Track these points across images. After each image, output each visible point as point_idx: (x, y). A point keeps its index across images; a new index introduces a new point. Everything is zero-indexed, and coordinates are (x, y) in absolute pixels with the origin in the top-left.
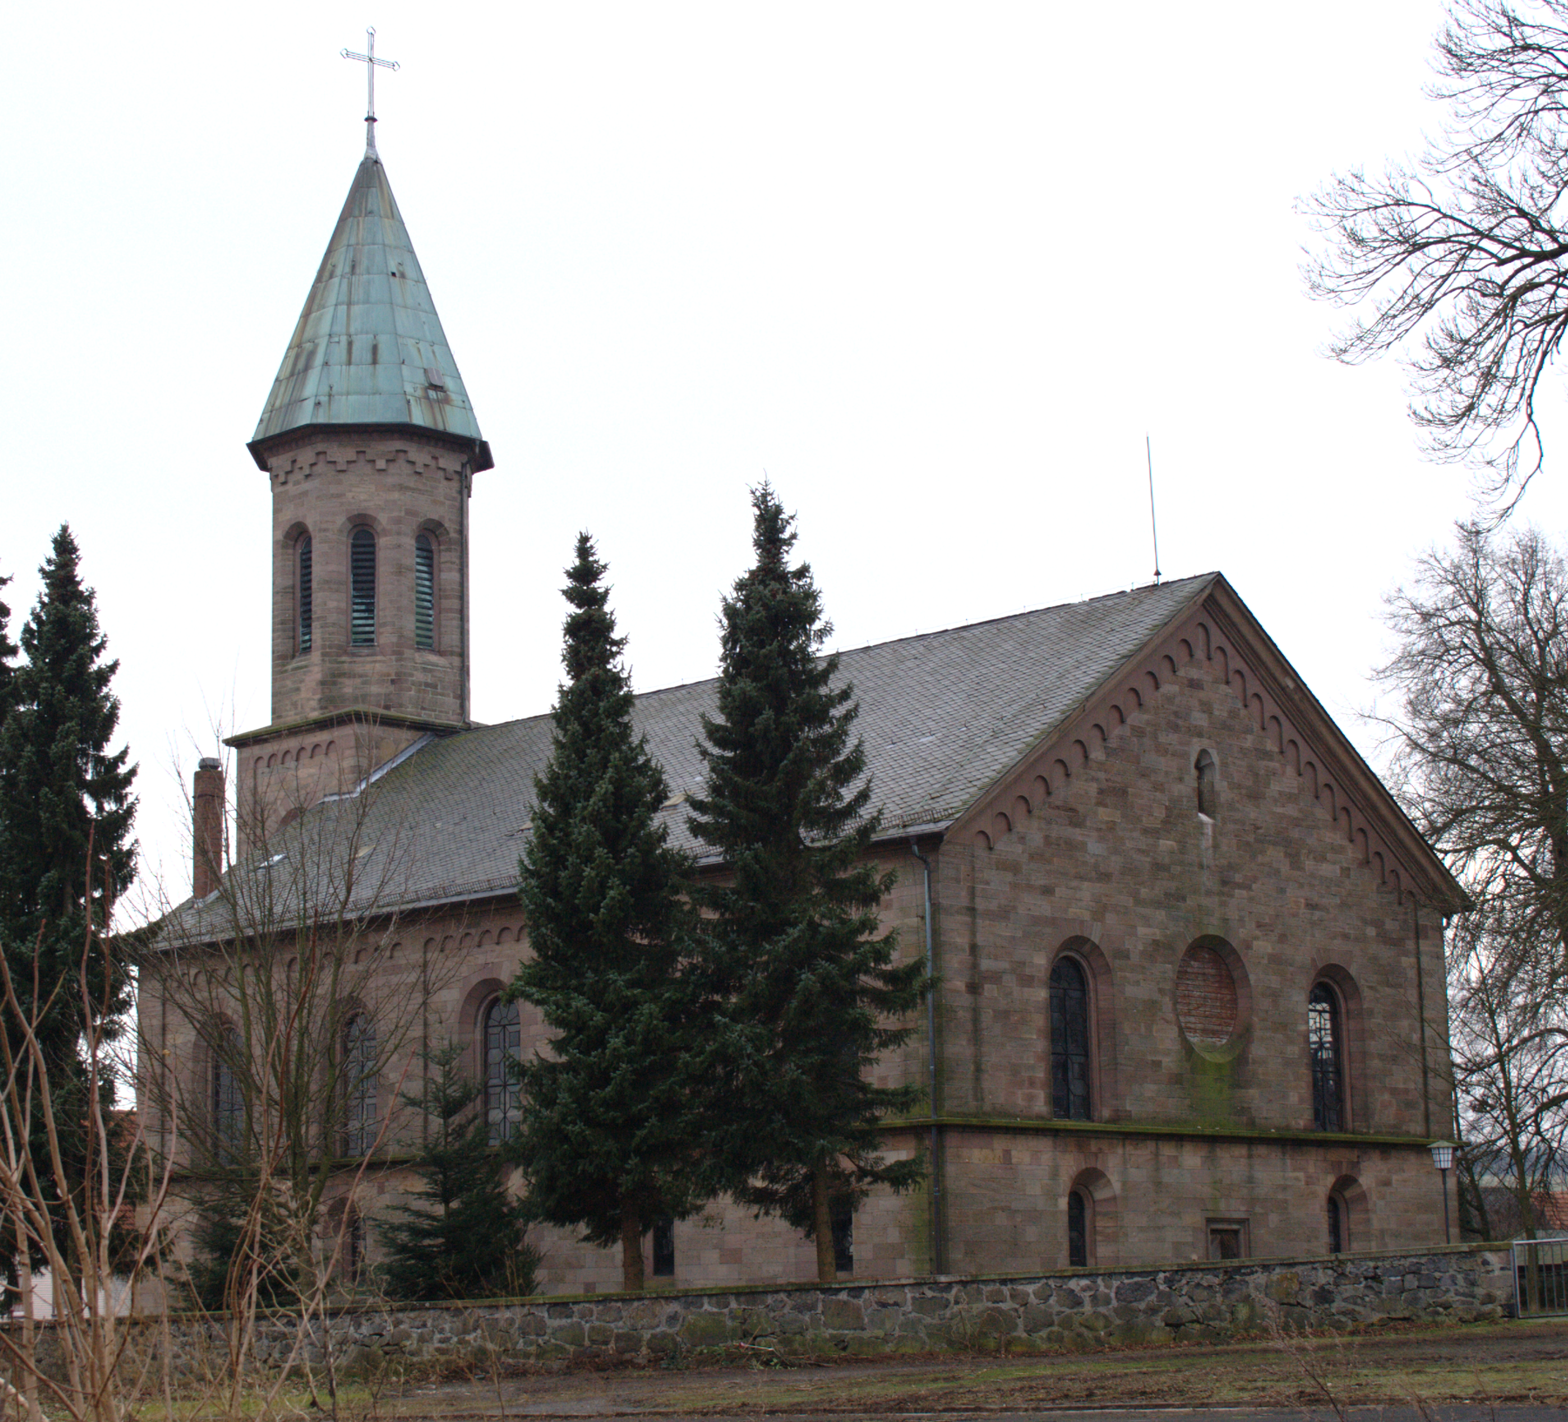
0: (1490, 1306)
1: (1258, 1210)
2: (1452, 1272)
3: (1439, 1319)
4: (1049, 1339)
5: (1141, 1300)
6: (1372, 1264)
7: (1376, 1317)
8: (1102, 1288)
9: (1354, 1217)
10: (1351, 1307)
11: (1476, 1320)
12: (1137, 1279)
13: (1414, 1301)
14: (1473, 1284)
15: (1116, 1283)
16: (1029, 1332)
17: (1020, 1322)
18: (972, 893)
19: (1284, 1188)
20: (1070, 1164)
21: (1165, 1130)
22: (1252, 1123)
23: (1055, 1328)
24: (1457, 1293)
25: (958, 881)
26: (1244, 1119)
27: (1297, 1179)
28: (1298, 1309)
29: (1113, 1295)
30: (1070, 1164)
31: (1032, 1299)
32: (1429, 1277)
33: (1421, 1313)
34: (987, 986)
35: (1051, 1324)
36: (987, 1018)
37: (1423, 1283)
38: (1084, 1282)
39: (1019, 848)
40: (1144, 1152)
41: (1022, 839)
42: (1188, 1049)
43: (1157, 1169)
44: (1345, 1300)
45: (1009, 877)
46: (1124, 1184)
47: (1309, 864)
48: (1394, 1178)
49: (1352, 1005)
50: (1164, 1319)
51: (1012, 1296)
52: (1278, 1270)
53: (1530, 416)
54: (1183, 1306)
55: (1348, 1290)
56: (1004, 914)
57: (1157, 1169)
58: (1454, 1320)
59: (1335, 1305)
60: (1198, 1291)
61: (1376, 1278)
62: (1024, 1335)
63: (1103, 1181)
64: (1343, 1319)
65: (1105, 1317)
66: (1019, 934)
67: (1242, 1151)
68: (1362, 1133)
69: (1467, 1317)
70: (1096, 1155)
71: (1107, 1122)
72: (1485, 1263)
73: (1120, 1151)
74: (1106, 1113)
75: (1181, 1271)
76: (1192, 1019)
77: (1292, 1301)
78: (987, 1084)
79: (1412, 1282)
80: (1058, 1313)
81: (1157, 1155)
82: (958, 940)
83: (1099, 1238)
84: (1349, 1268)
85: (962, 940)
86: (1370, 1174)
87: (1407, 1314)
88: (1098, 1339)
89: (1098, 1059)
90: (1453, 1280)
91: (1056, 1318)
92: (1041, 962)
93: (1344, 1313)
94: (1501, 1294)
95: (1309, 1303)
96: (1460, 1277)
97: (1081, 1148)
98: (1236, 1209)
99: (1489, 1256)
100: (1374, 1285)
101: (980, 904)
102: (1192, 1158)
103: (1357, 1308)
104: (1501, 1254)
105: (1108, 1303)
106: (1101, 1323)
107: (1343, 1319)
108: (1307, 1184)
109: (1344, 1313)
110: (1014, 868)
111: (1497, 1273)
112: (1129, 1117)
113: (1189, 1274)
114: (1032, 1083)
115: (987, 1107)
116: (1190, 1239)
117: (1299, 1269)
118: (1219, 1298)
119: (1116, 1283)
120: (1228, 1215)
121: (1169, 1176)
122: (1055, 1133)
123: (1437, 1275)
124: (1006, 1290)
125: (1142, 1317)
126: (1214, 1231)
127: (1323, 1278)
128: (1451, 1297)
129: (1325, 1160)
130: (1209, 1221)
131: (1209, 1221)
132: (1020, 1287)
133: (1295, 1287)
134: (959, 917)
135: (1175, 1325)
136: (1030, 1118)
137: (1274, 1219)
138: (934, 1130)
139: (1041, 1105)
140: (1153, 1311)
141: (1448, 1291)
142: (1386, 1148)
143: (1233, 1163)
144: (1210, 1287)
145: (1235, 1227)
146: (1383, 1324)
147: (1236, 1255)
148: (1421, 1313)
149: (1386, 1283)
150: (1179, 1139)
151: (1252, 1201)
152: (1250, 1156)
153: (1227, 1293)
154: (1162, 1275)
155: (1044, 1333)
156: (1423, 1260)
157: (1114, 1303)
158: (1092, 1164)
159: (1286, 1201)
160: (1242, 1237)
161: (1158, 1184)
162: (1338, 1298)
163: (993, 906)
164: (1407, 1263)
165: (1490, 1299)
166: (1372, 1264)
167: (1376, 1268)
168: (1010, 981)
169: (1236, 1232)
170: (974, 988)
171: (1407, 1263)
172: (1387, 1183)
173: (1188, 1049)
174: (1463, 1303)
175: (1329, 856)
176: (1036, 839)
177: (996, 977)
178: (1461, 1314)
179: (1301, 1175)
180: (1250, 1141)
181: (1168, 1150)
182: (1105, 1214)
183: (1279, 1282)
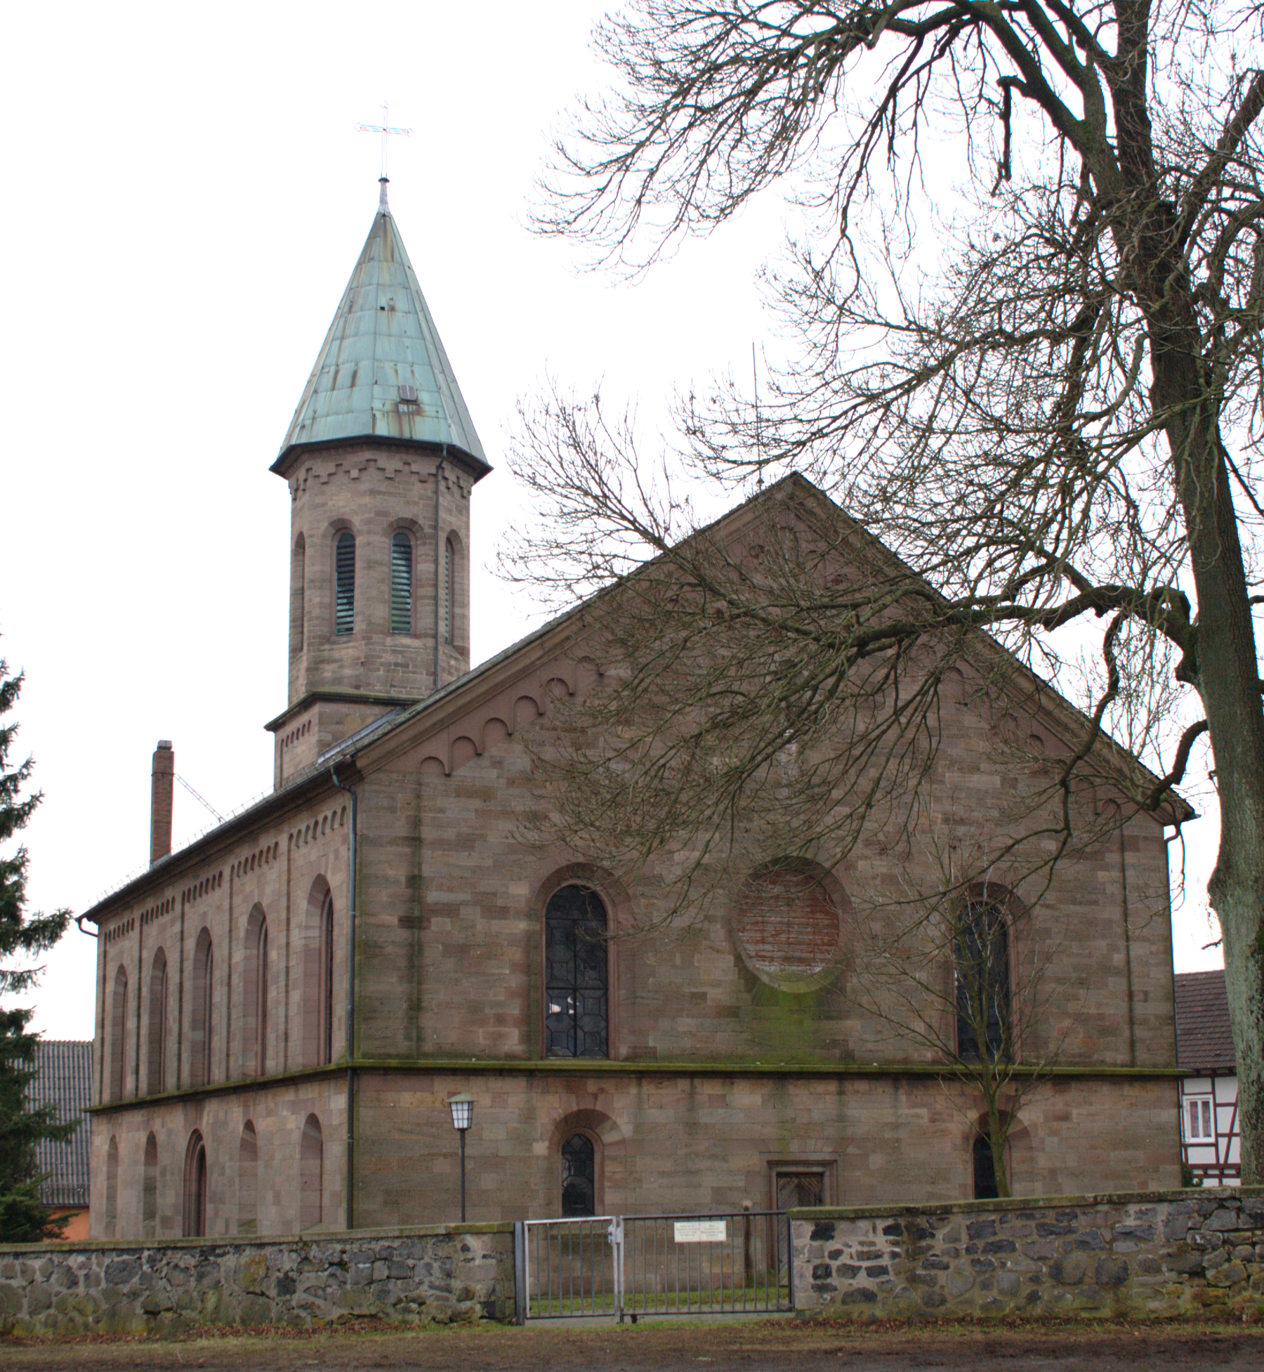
0: (468, 1304)
1: (851, 1150)
2: (427, 1260)
3: (410, 1317)
4: (46, 1324)
5: (125, 1282)
6: (338, 1247)
7: (335, 1313)
8: (94, 1267)
9: (1017, 1154)
10: (312, 1299)
11: (451, 1320)
12: (125, 1257)
13: (383, 1294)
14: (449, 1275)
15: (107, 1261)
16: (32, 1313)
17: (25, 1301)
18: (416, 823)
19: (896, 1126)
20: (552, 1106)
21: (709, 1066)
22: (848, 1056)
23: (52, 1311)
24: (432, 1287)
25: (392, 810)
26: (837, 1052)
27: (917, 1116)
28: (261, 1300)
29: (103, 1274)
30: (552, 1106)
31: (38, 1277)
32: (401, 1265)
33: (390, 1310)
34: (433, 920)
35: (49, 1307)
36: (432, 953)
37: (394, 1273)
38: (81, 1258)
39: (494, 773)
40: (674, 1092)
41: (498, 764)
42: (750, 980)
43: (691, 1109)
44: (307, 1290)
45: (477, 803)
46: (638, 1127)
47: (951, 777)
48: (1075, 1112)
49: (1021, 924)
50: (143, 1306)
51: (23, 1272)
52: (248, 1252)
53: (843, 231)
54: (166, 1293)
55: (311, 1278)
56: (466, 843)
57: (691, 1109)
58: (426, 1319)
59: (296, 1296)
60: (176, 1273)
61: (342, 1265)
62: (27, 1317)
63: (608, 1124)
64: (303, 1314)
65: (95, 1300)
66: (490, 863)
67: (832, 1086)
68: (1031, 1064)
69: (440, 1317)
70: (595, 1096)
71: (626, 1059)
72: (465, 1248)
73: (633, 1090)
74: (623, 1050)
75: (163, 1249)
76: (768, 947)
77: (258, 1290)
78: (429, 1021)
79: (381, 1270)
80: (58, 1294)
81: (692, 1095)
82: (390, 873)
83: (607, 1184)
84: (314, 1252)
85: (398, 872)
86: (1033, 1111)
87: (373, 1310)
88: (86, 1325)
89: (618, 993)
90: (428, 1267)
91: (54, 1299)
92: (520, 891)
93: (303, 1307)
94: (480, 1289)
95: (273, 1292)
96: (436, 1265)
97: (569, 1089)
98: (818, 1150)
99: (471, 1241)
100: (339, 1273)
101: (427, 833)
102: (747, 1097)
103: (318, 1302)
104: (485, 1238)
105: (98, 1283)
106: (90, 1308)
107: (303, 1314)
108: (933, 1120)
109: (303, 1307)
110: (486, 794)
111: (477, 1262)
112: (652, 1054)
113: (169, 1253)
114: (500, 1020)
115: (428, 1047)
116: (741, 1184)
117: (268, 1250)
118: (193, 1283)
119: (107, 1261)
120: (803, 1157)
121: (707, 1116)
122: (530, 1073)
123: (410, 1262)
124: (17, 1264)
125: (125, 1300)
126: (779, 1175)
127: (288, 1262)
128: (424, 1291)
129: (963, 1094)
130: (771, 1164)
131: (771, 1164)
132: (30, 1262)
133: (262, 1272)
134: (389, 848)
135: (152, 1313)
136: (496, 1058)
137: (877, 1160)
138: (349, 1073)
139: (512, 1042)
140: (134, 1295)
141: (421, 1283)
142: (1062, 1081)
143: (812, 1103)
144: (187, 1268)
145: (819, 1169)
146: (343, 1320)
147: (820, 1201)
148: (390, 1310)
149: (352, 1270)
150: (728, 1076)
151: (843, 1141)
152: (841, 1093)
153: (201, 1276)
154: (146, 1253)
155: (42, 1317)
156: (396, 1244)
157: (104, 1285)
158: (587, 1104)
159: (898, 1140)
160: (827, 1180)
161: (692, 1127)
162: (300, 1288)
163: (450, 834)
164: (377, 1246)
165: (467, 1294)
166: (338, 1247)
167: (343, 1252)
168: (472, 914)
169: (821, 1175)
170: (412, 922)
171: (377, 1246)
172: (1065, 1117)
173: (750, 980)
174: (438, 1298)
175: (982, 766)
176: (519, 761)
177: (450, 910)
178: (434, 1312)
179: (924, 1112)
180: (841, 1077)
181: (709, 1089)
182: (613, 1159)
183: (248, 1265)
